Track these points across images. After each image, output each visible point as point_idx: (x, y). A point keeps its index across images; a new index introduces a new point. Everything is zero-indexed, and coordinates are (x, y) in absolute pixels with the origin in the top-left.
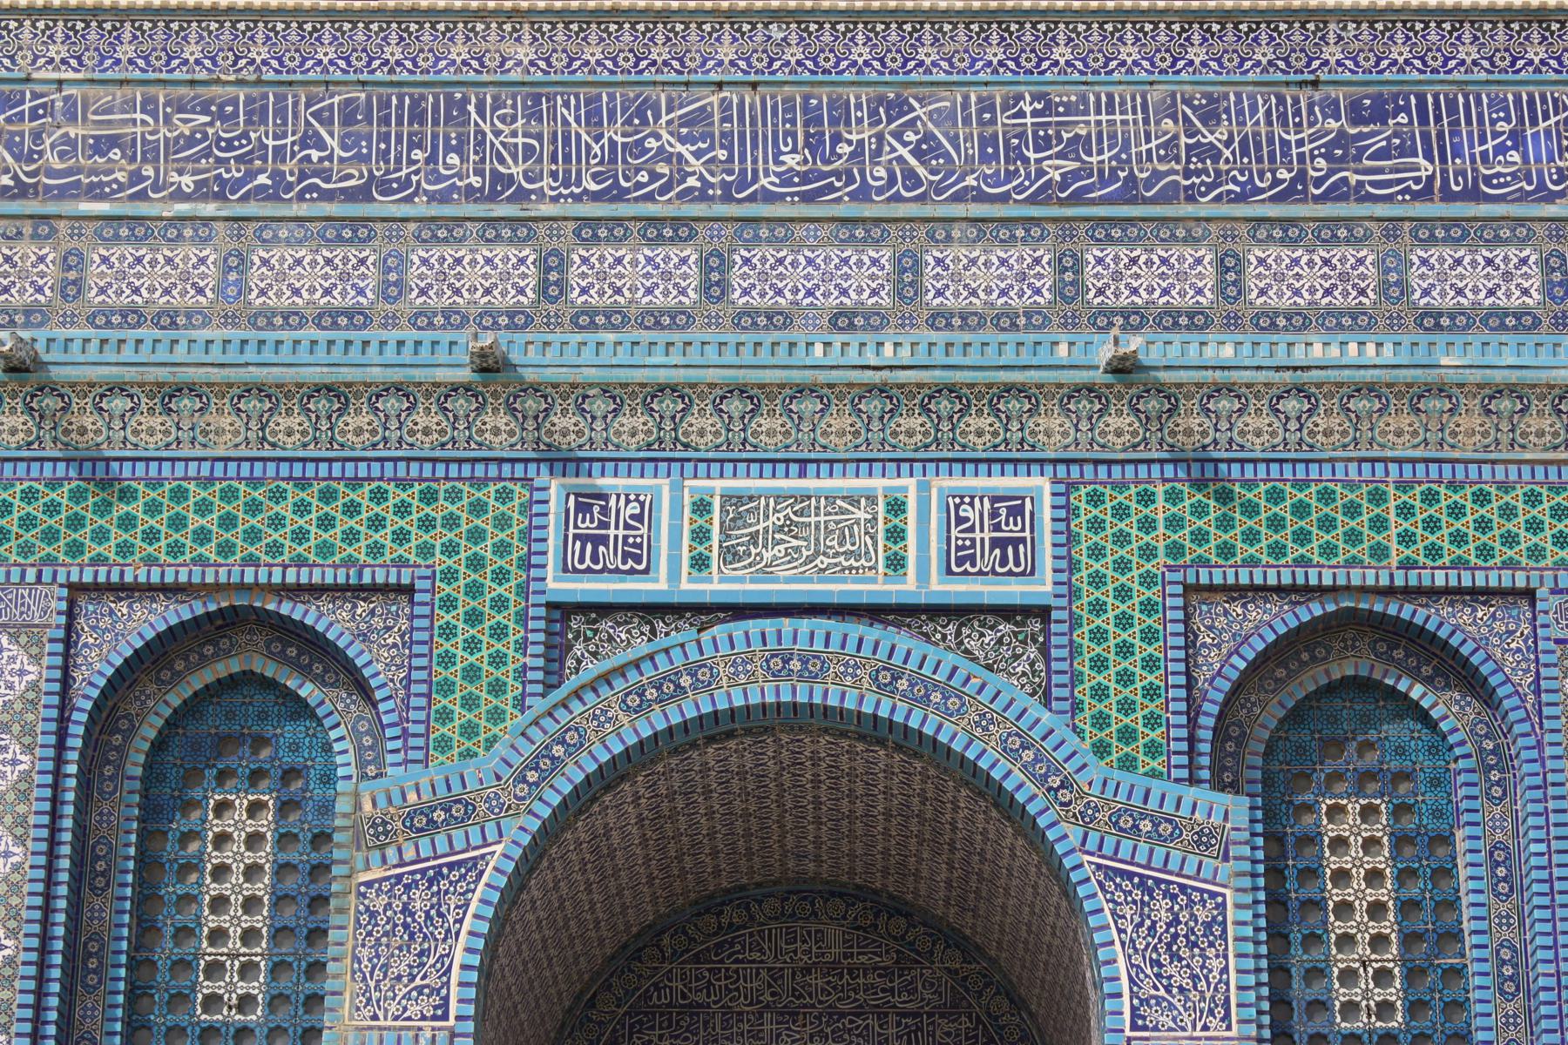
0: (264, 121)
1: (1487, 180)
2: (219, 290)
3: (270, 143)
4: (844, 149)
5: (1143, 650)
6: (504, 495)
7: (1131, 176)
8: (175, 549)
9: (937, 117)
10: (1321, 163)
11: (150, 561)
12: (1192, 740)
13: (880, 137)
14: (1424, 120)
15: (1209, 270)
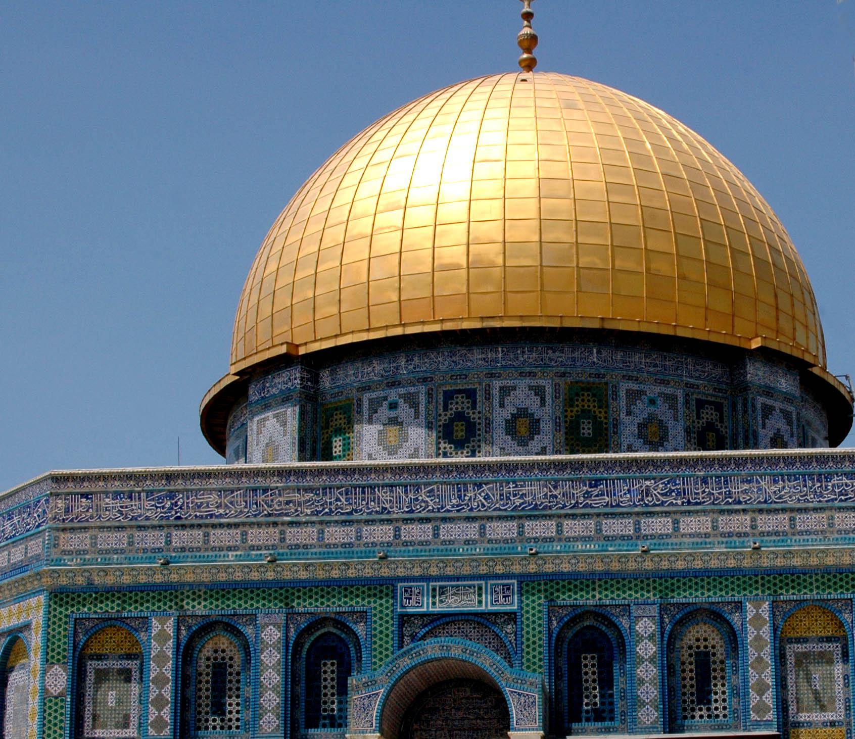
0: (326, 495)
1: (621, 502)
2: (318, 539)
3: (328, 501)
4: (467, 498)
5: (538, 622)
6: (387, 588)
7: (536, 503)
8: (311, 604)
9: (491, 489)
10: (582, 498)
11: (305, 607)
12: (550, 643)
13: (475, 495)
14: (607, 487)
15: (554, 527)
